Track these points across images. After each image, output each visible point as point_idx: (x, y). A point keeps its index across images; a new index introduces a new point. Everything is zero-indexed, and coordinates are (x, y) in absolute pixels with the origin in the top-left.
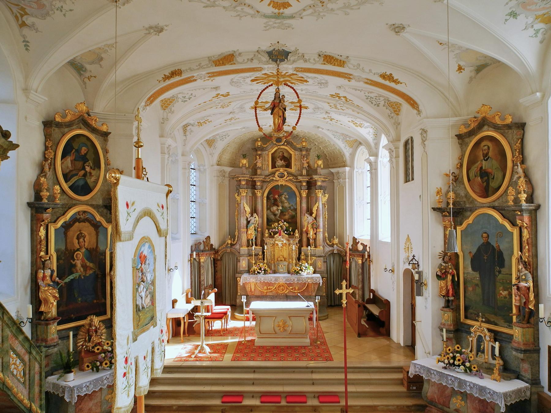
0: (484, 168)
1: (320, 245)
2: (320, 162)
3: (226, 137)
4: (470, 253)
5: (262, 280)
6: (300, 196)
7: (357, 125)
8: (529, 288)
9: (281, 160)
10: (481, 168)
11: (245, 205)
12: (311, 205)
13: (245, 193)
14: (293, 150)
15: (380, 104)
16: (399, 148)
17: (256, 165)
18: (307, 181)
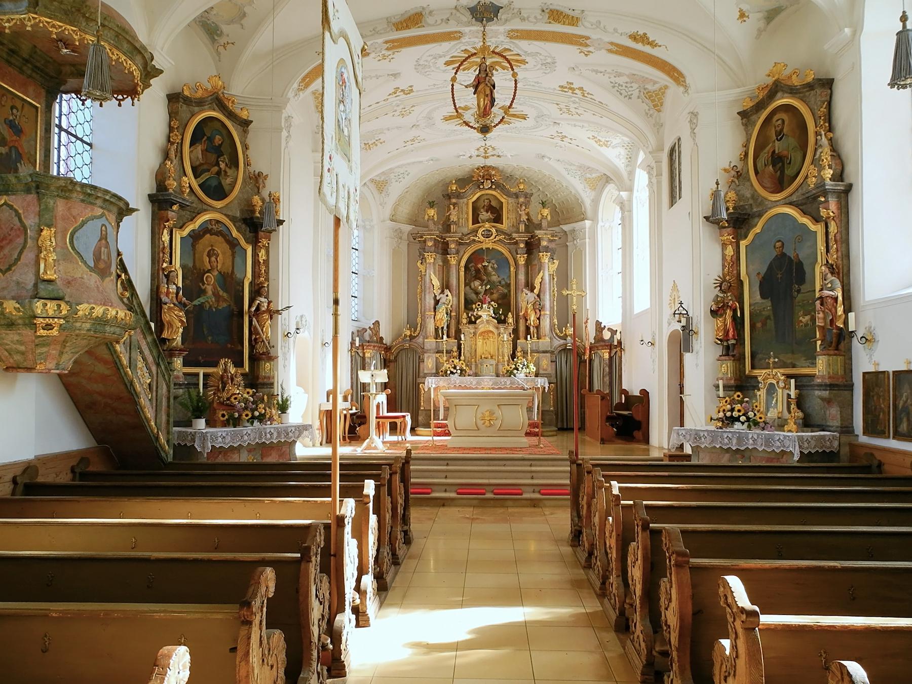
0: (777, 152)
1: (545, 336)
2: (546, 212)
3: (405, 176)
4: (759, 274)
6: (516, 265)
7: (601, 143)
8: (836, 299)
9: (487, 212)
10: (774, 152)
11: (433, 276)
12: (532, 277)
13: (433, 259)
14: (505, 197)
15: (632, 94)
16: (661, 162)
17: (448, 218)
18: (526, 240)
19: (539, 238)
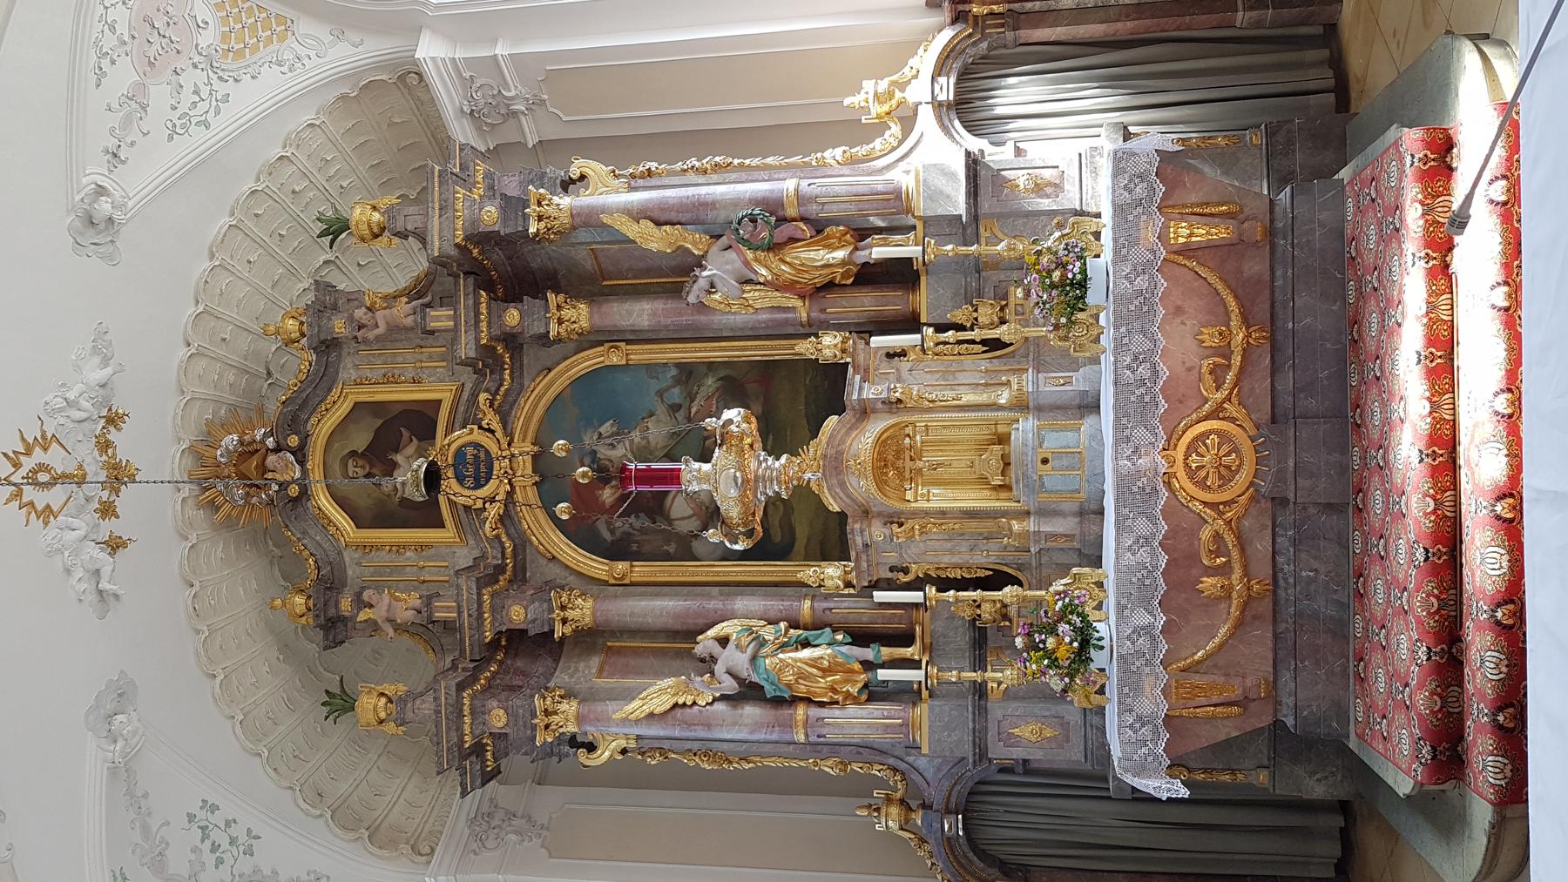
3: (218, 818)
5: (1148, 619)
6: (601, 343)
11: (636, 708)
12: (647, 272)
13: (564, 706)
14: (335, 392)
19: (467, 238)
